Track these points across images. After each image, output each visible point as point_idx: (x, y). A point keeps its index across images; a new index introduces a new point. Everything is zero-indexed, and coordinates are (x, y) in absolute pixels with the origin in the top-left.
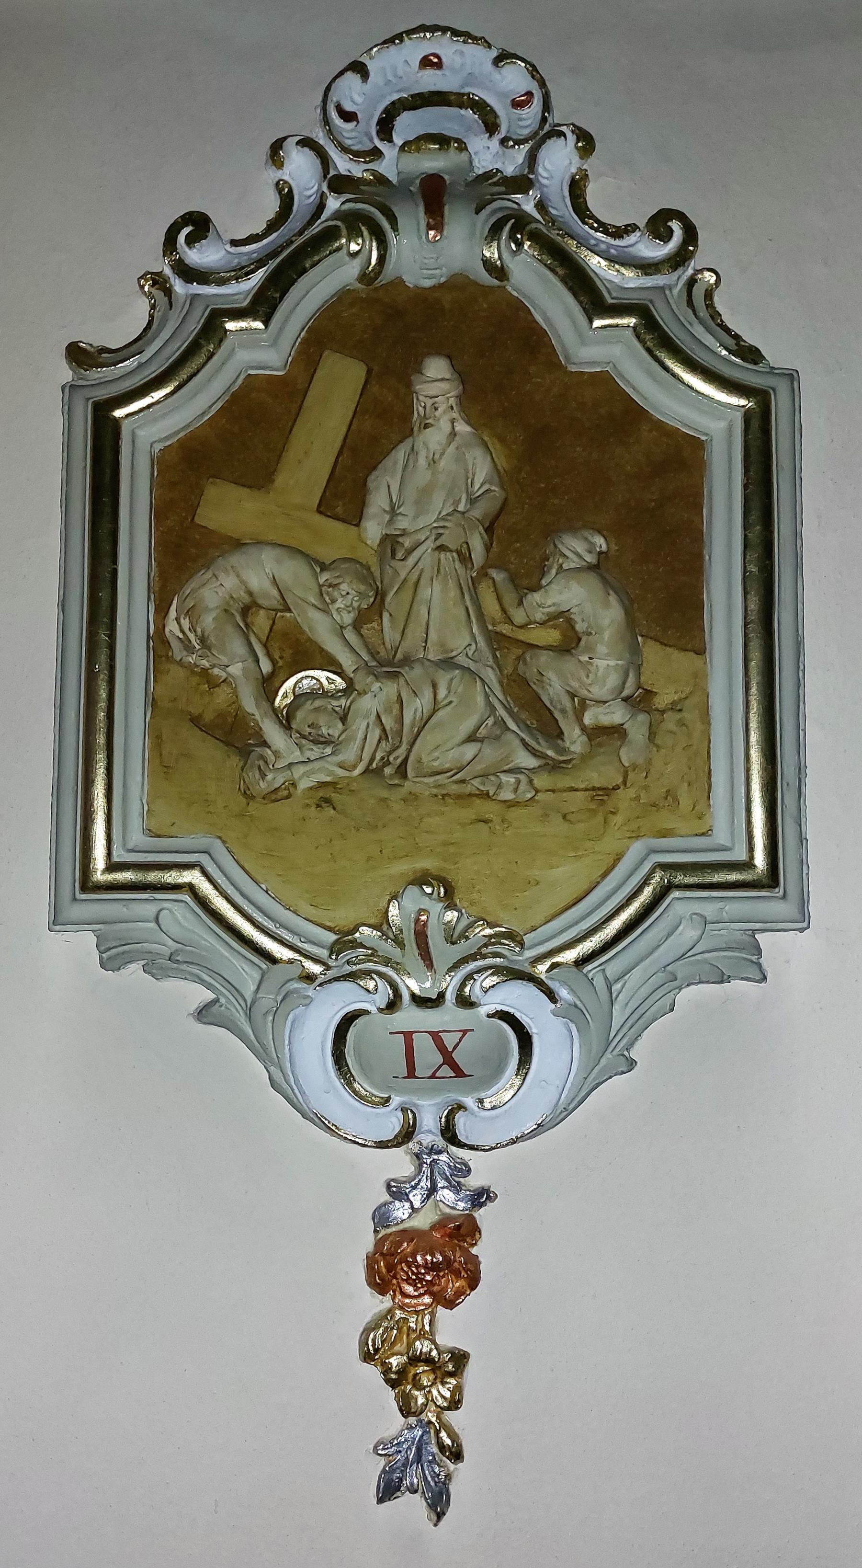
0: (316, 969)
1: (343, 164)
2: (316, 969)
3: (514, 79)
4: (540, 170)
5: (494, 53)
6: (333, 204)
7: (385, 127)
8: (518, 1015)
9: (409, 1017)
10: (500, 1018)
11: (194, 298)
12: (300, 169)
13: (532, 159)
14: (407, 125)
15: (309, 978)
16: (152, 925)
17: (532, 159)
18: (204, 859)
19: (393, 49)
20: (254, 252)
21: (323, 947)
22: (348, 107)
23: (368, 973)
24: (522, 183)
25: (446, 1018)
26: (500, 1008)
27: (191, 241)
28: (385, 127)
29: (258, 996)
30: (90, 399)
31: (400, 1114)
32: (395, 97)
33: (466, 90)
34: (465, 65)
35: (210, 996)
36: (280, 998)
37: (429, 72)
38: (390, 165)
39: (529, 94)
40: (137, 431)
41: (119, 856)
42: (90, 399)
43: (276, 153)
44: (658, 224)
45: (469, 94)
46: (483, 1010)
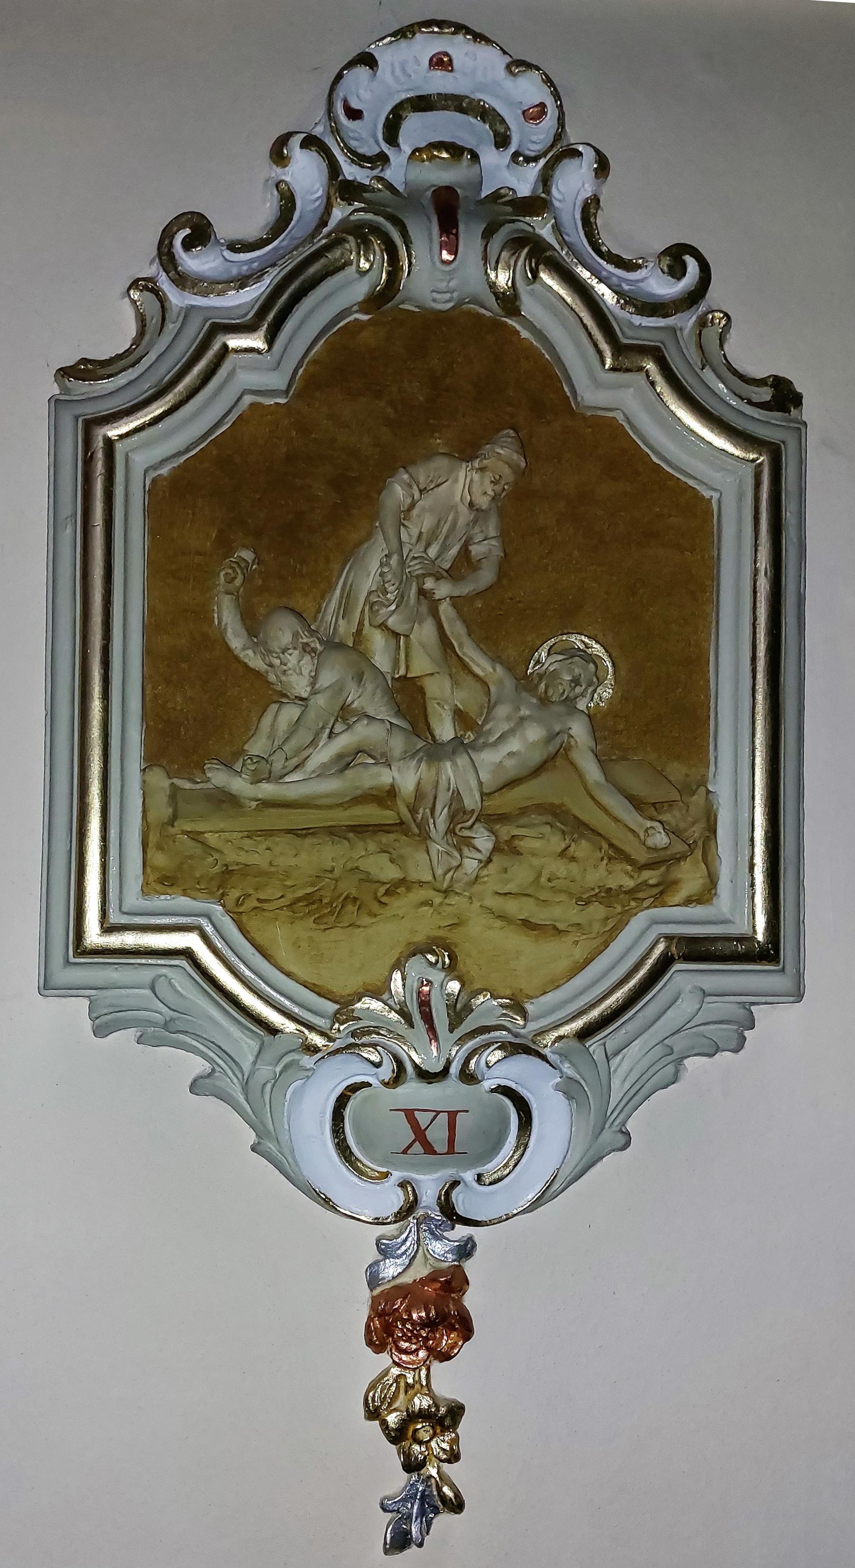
0: (318, 1040)
1: (350, 171)
2: (318, 1040)
3: (529, 90)
4: (554, 191)
5: (508, 59)
6: (338, 213)
7: (392, 130)
8: (519, 1089)
9: (413, 1092)
10: (502, 1093)
11: (190, 310)
12: (305, 173)
13: (546, 179)
14: (417, 129)
15: (312, 1050)
16: (147, 992)
17: (546, 179)
18: (204, 922)
19: (403, 43)
20: (252, 261)
21: (322, 1016)
22: (355, 104)
23: (374, 1045)
24: (536, 204)
25: (448, 1094)
26: (504, 1082)
27: (188, 245)
28: (392, 130)
29: (256, 1067)
30: (79, 416)
31: (400, 1191)
32: (404, 96)
33: (478, 96)
34: (477, 68)
35: (206, 1066)
36: (278, 1069)
37: (439, 74)
38: (397, 172)
39: (542, 105)
40: (130, 454)
41: (115, 918)
42: (79, 416)
43: (278, 154)
44: (675, 258)
45: (480, 100)
46: (489, 1084)
